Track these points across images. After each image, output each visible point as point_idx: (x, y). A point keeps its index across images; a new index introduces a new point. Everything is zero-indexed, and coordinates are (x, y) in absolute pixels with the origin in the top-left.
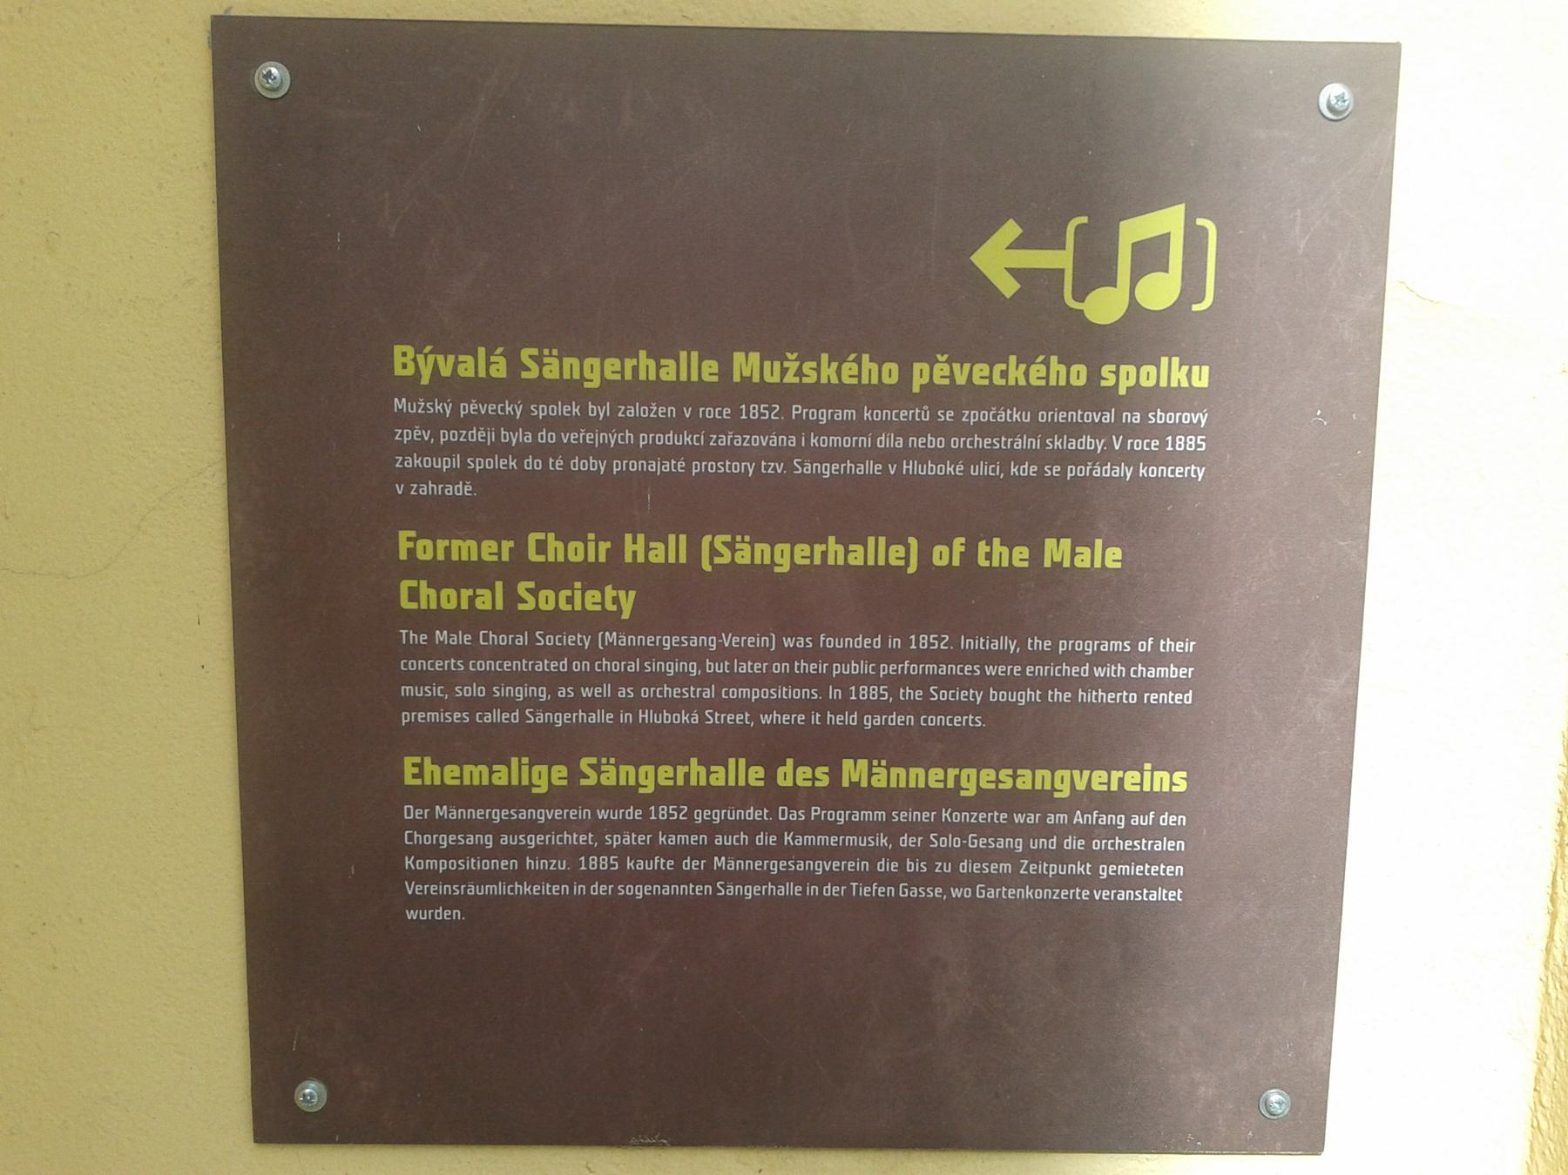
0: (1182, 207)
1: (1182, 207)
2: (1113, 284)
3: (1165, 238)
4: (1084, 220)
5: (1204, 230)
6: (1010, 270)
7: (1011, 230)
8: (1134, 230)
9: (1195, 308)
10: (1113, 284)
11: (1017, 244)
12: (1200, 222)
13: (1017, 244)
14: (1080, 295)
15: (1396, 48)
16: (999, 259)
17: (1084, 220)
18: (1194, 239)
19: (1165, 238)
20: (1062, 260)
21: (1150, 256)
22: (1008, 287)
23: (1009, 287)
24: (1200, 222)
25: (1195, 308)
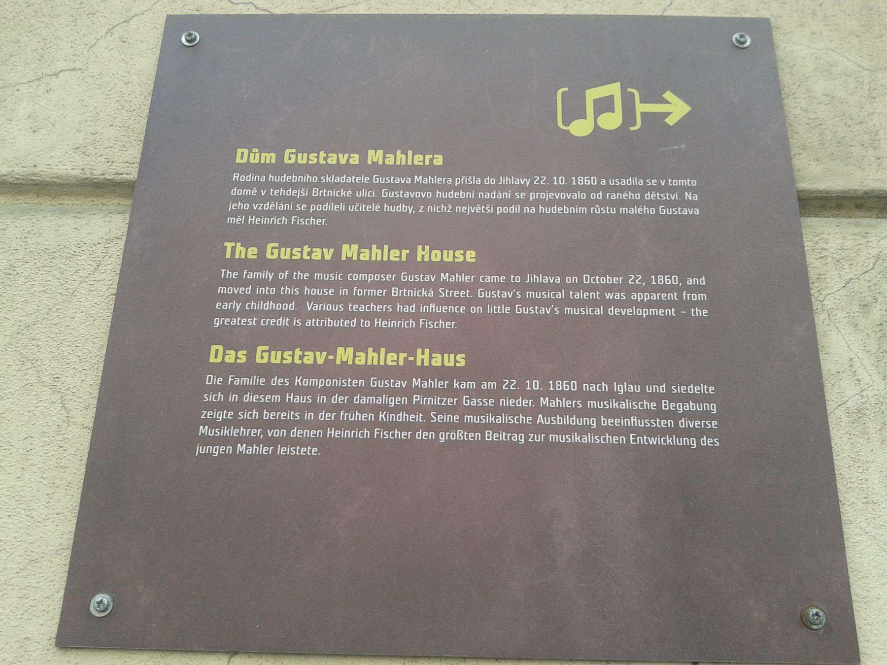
3: (611, 98)
5: (632, 94)
12: (629, 90)
14: (567, 122)
19: (611, 98)
24: (629, 90)
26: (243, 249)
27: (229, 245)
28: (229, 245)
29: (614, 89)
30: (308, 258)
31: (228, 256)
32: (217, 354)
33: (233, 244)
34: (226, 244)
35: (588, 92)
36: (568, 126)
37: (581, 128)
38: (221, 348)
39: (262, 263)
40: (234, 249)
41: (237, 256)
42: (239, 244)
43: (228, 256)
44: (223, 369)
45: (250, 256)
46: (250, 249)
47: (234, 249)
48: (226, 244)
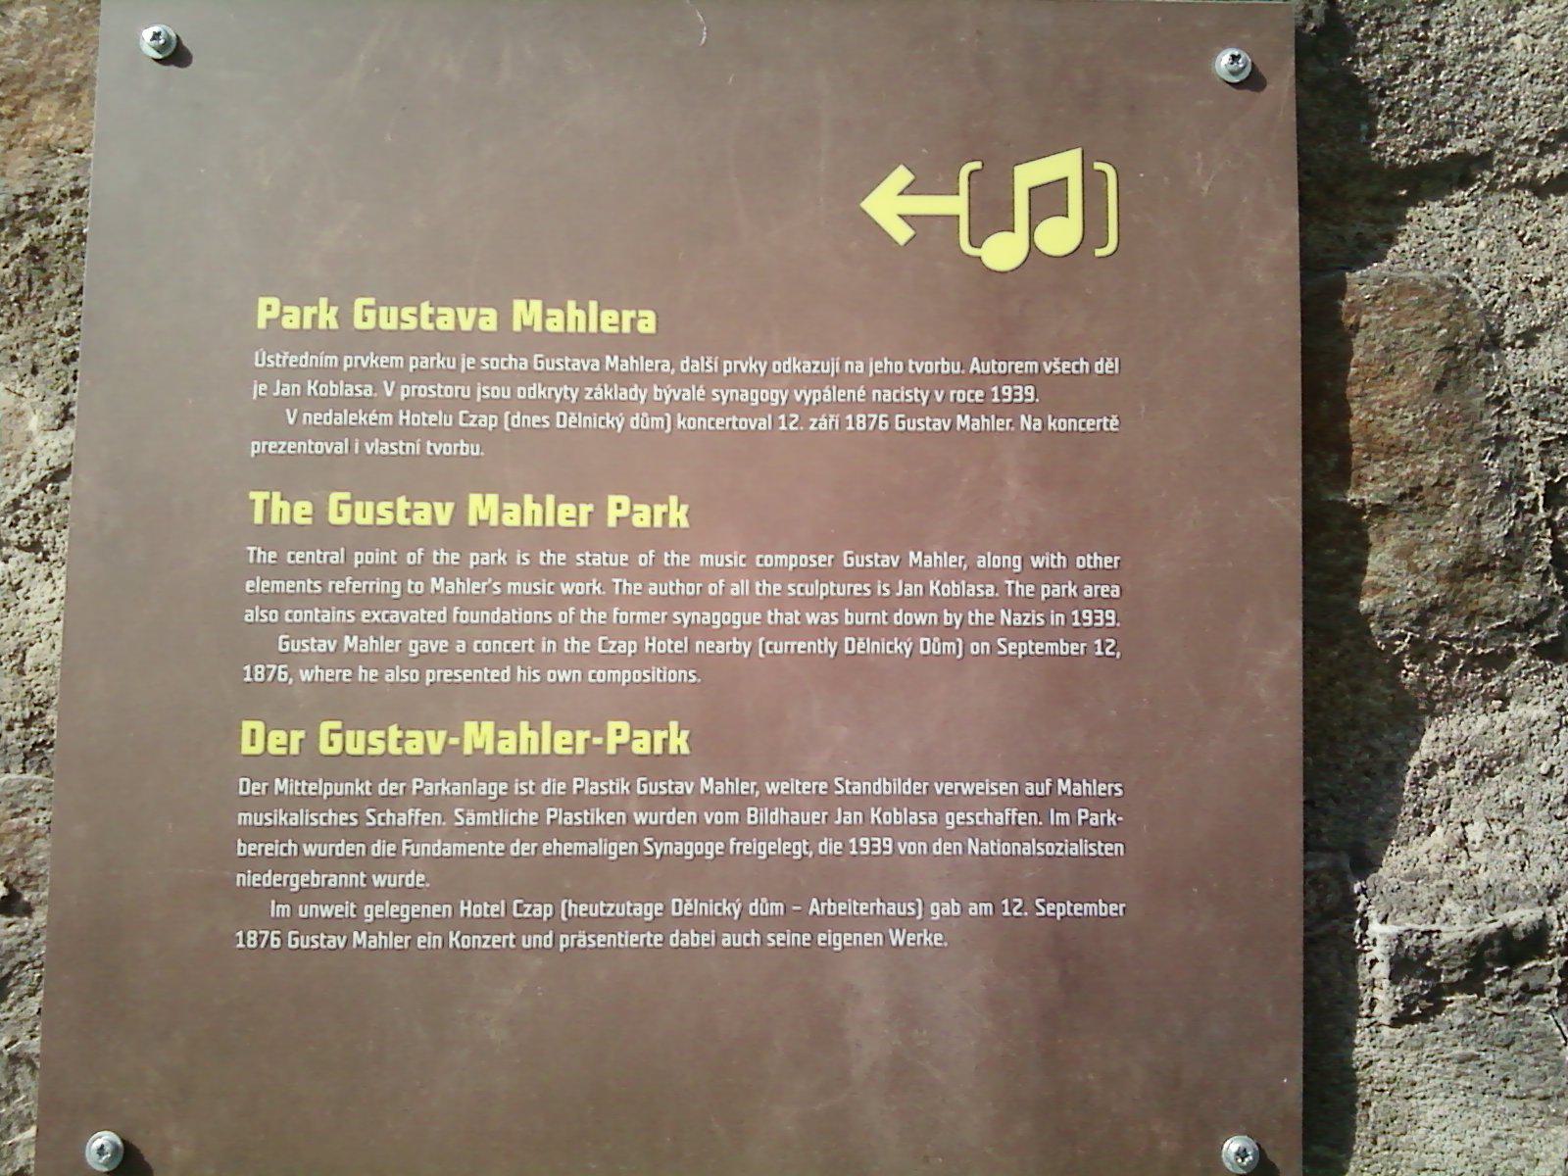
4: (977, 165)
6: (900, 216)
7: (901, 176)
8: (1029, 175)
9: (1099, 252)
11: (908, 190)
12: (1098, 166)
13: (908, 190)
14: (975, 242)
16: (890, 204)
17: (977, 165)
18: (1092, 184)
20: (956, 205)
21: (1048, 200)
22: (902, 233)
23: (902, 233)
24: (1098, 166)
25: (1099, 252)
26: (286, 505)
27: (258, 497)
28: (258, 497)
29: (1066, 165)
31: (258, 519)
32: (255, 738)
33: (266, 495)
34: (253, 495)
35: (1018, 169)
36: (980, 247)
37: (1003, 252)
38: (259, 726)
39: (320, 532)
40: (267, 503)
41: (275, 520)
42: (276, 495)
43: (258, 519)
44: (267, 766)
45: (299, 520)
46: (298, 505)
47: (267, 503)
48: (253, 495)
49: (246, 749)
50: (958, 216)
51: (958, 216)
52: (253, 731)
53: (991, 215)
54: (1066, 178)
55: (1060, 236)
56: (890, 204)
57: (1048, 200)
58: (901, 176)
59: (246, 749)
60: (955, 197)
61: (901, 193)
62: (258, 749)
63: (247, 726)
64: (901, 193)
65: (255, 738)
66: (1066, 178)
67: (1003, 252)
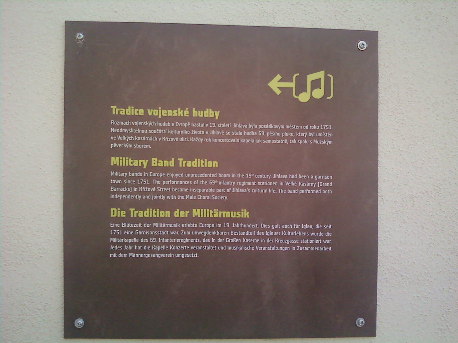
0: (324, 71)
1: (324, 71)
2: (306, 91)
4: (298, 74)
7: (279, 77)
8: (311, 77)
9: (328, 98)
10: (306, 91)
11: (280, 81)
12: (329, 75)
13: (280, 81)
14: (297, 94)
15: (377, 32)
16: (275, 84)
17: (298, 74)
18: (327, 80)
20: (292, 85)
21: (316, 84)
22: (278, 92)
23: (278, 92)
24: (329, 75)
25: (328, 98)
29: (320, 75)
30: (132, 165)
36: (298, 96)
37: (304, 97)
49: (112, 215)
50: (293, 88)
51: (293, 88)
52: (114, 211)
53: (301, 88)
54: (321, 78)
55: (318, 93)
56: (275, 84)
57: (316, 84)
58: (279, 77)
59: (112, 215)
60: (292, 83)
61: (278, 82)
62: (115, 215)
63: (112, 210)
64: (278, 82)
65: (114, 212)
66: (321, 78)
67: (304, 97)
